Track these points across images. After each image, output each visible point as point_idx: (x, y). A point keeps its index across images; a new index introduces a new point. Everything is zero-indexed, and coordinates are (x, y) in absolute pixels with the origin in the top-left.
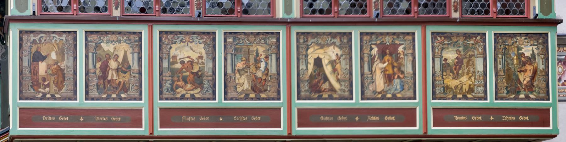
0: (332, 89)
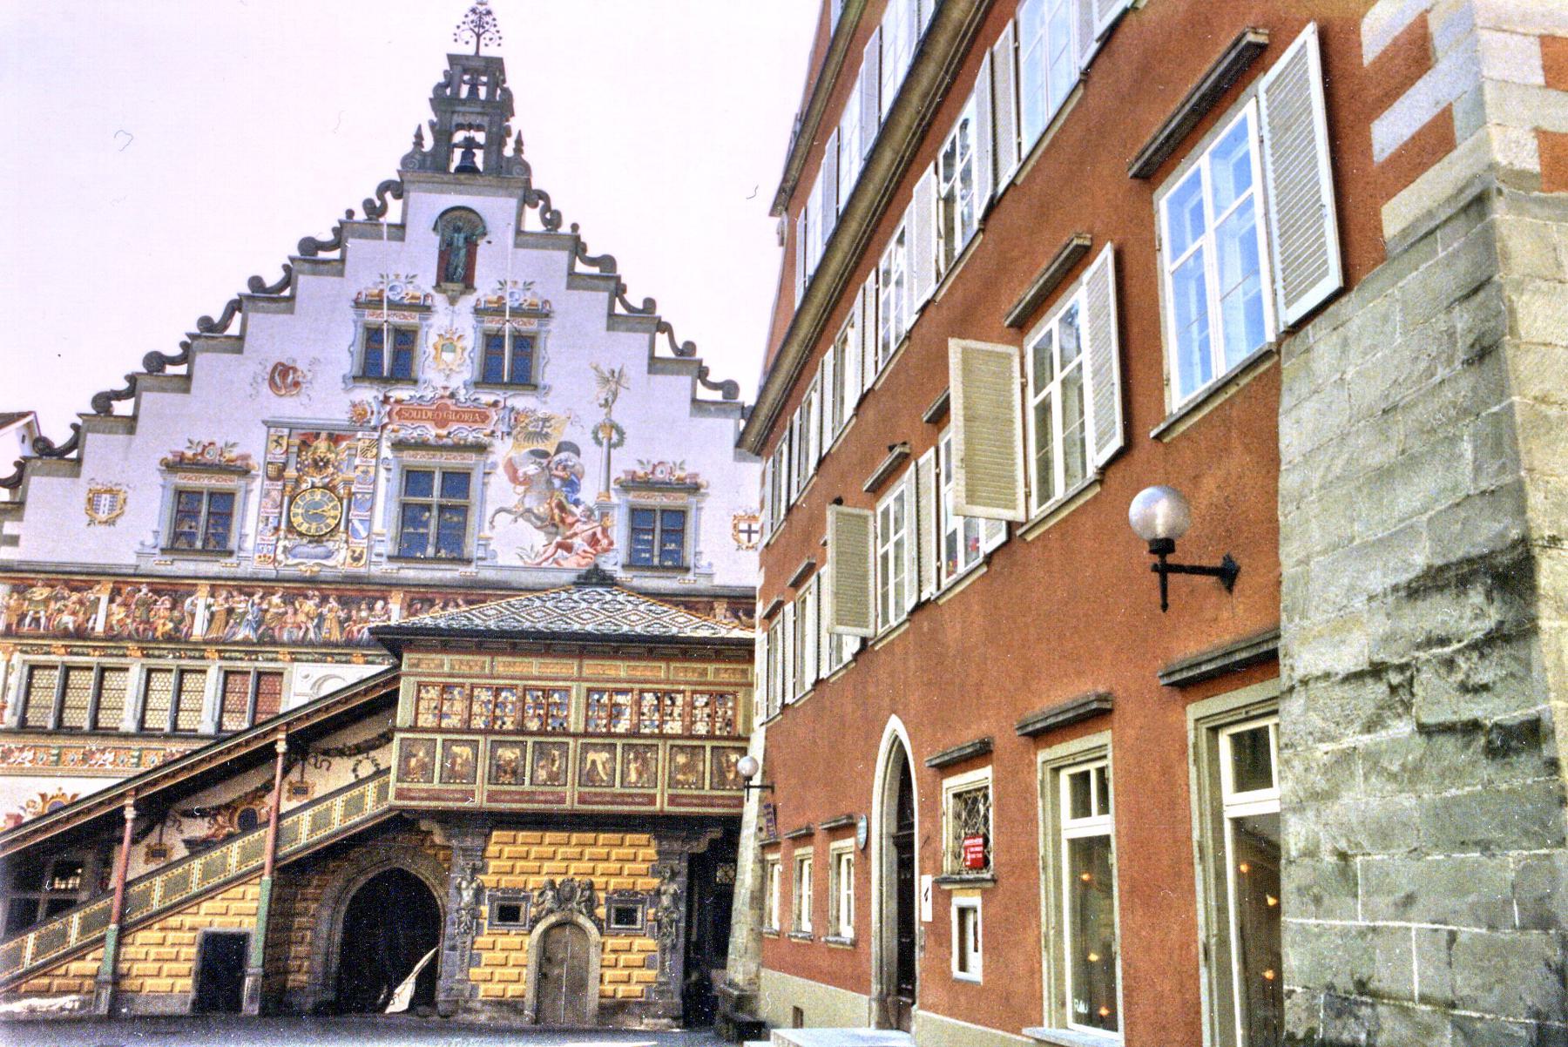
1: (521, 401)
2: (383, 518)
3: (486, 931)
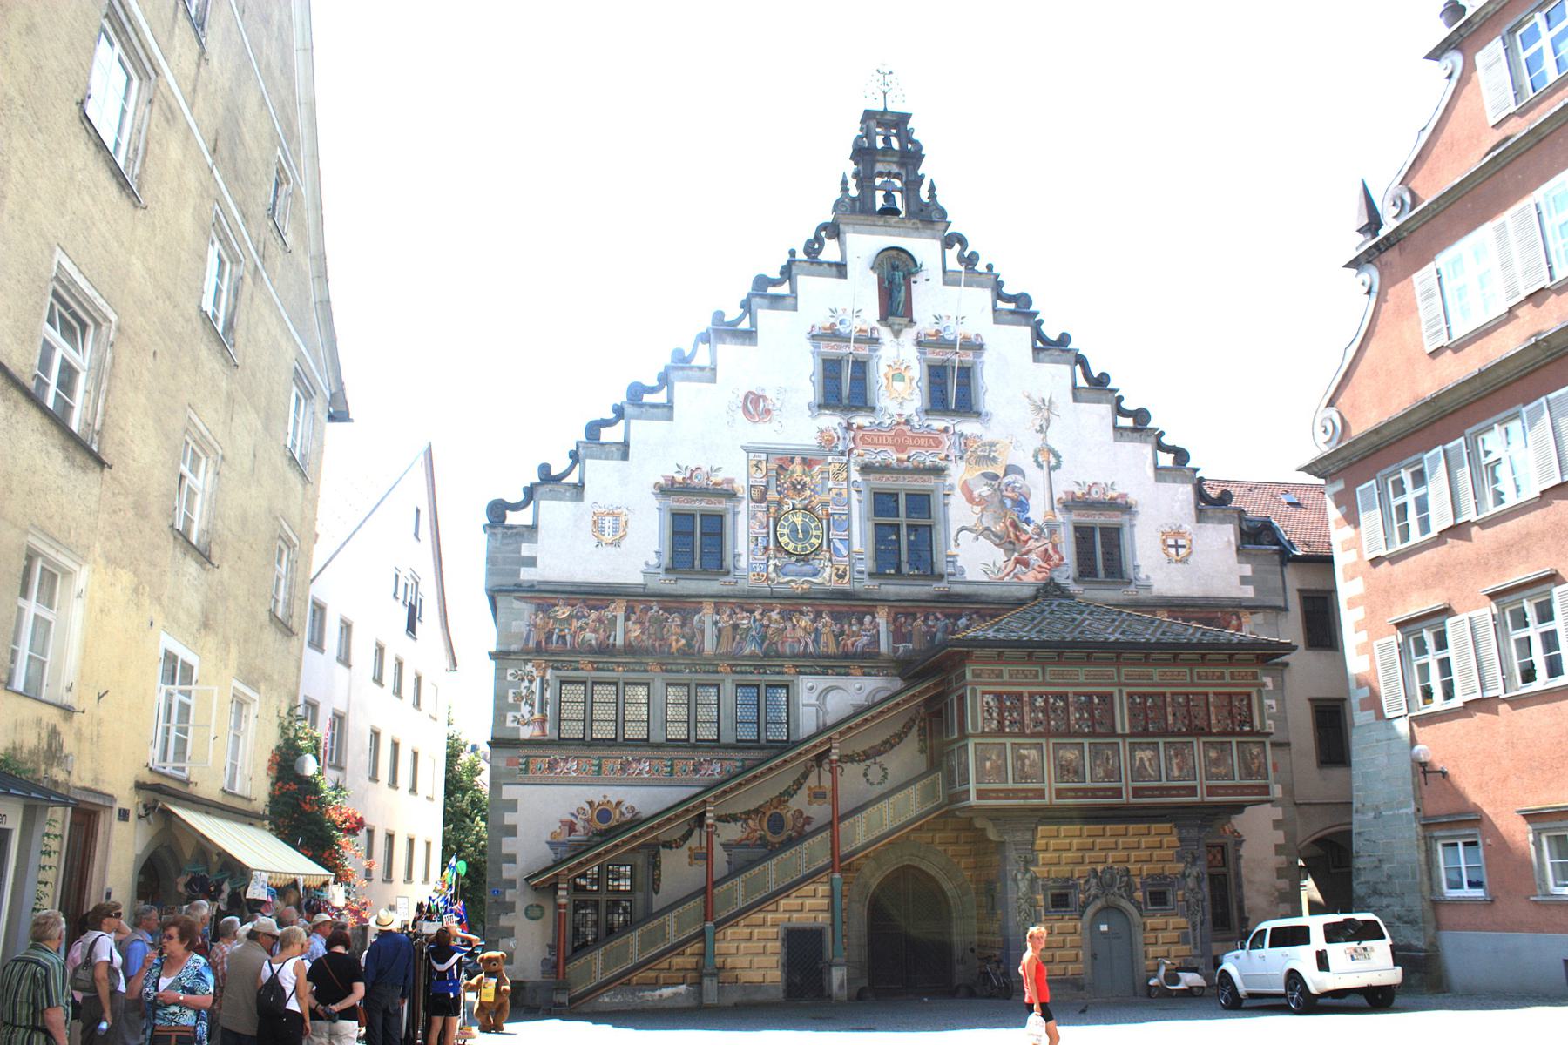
0: (1150, 776)
1: (969, 427)
2: (860, 535)
3: (1043, 918)
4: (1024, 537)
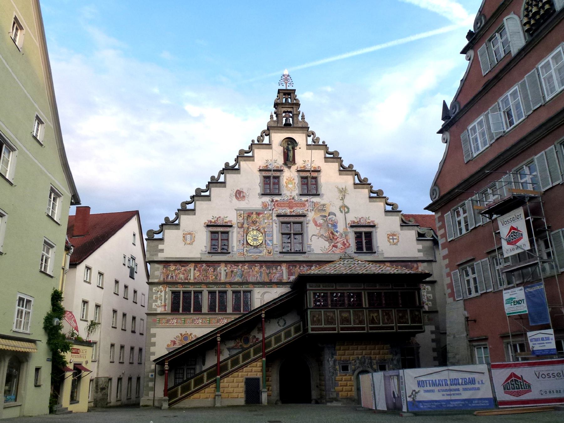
1: (315, 199)
2: (276, 237)
3: (339, 375)
4: (335, 237)
